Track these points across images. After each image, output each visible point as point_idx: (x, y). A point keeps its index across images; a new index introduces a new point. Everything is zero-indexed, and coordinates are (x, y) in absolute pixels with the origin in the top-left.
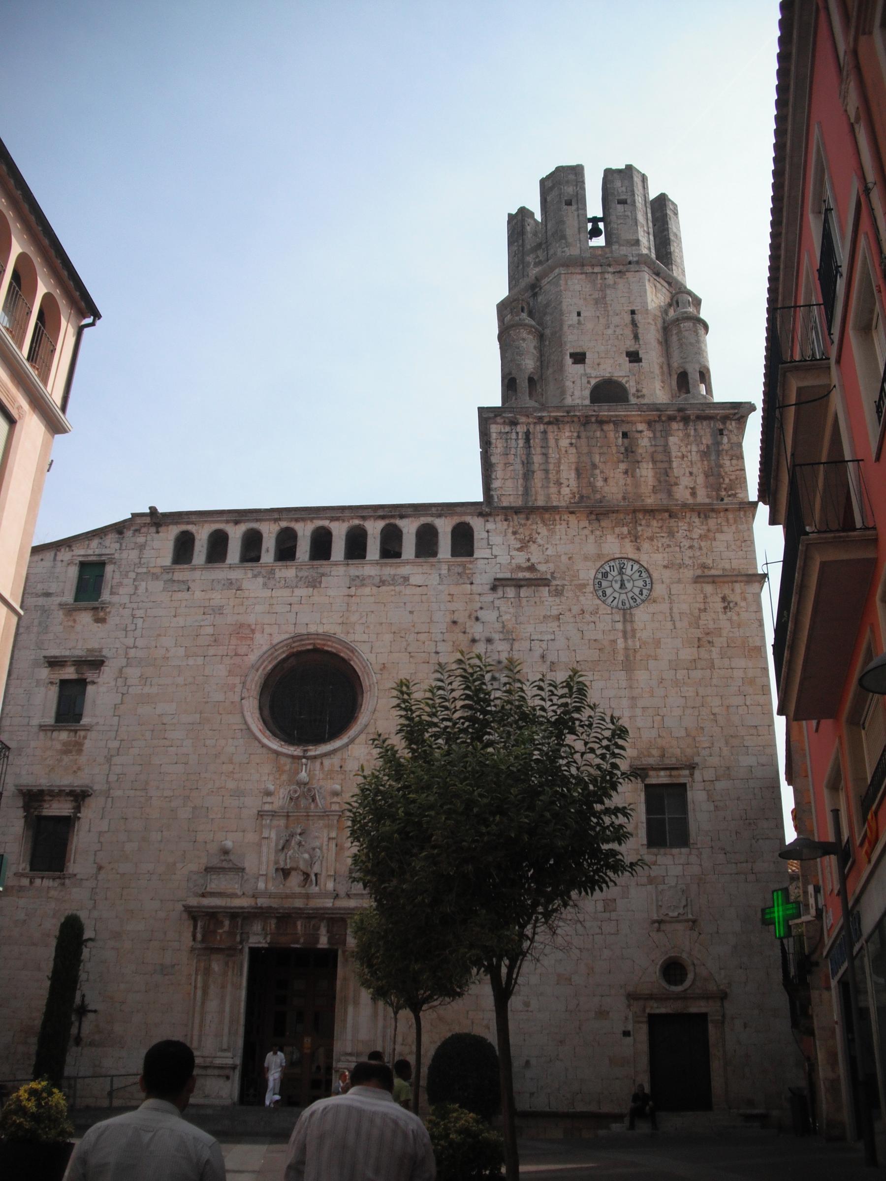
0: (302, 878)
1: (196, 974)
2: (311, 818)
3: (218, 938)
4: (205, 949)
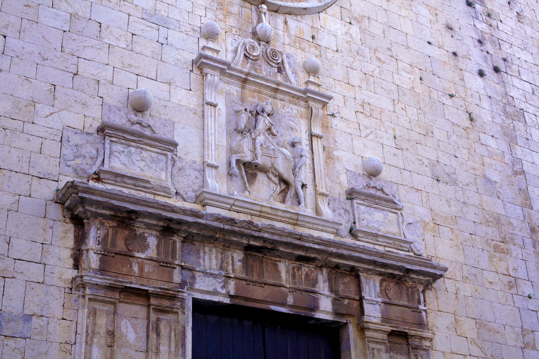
0: (279, 190)
1: (89, 344)
2: (279, 96)
3: (136, 268)
4: (111, 288)
